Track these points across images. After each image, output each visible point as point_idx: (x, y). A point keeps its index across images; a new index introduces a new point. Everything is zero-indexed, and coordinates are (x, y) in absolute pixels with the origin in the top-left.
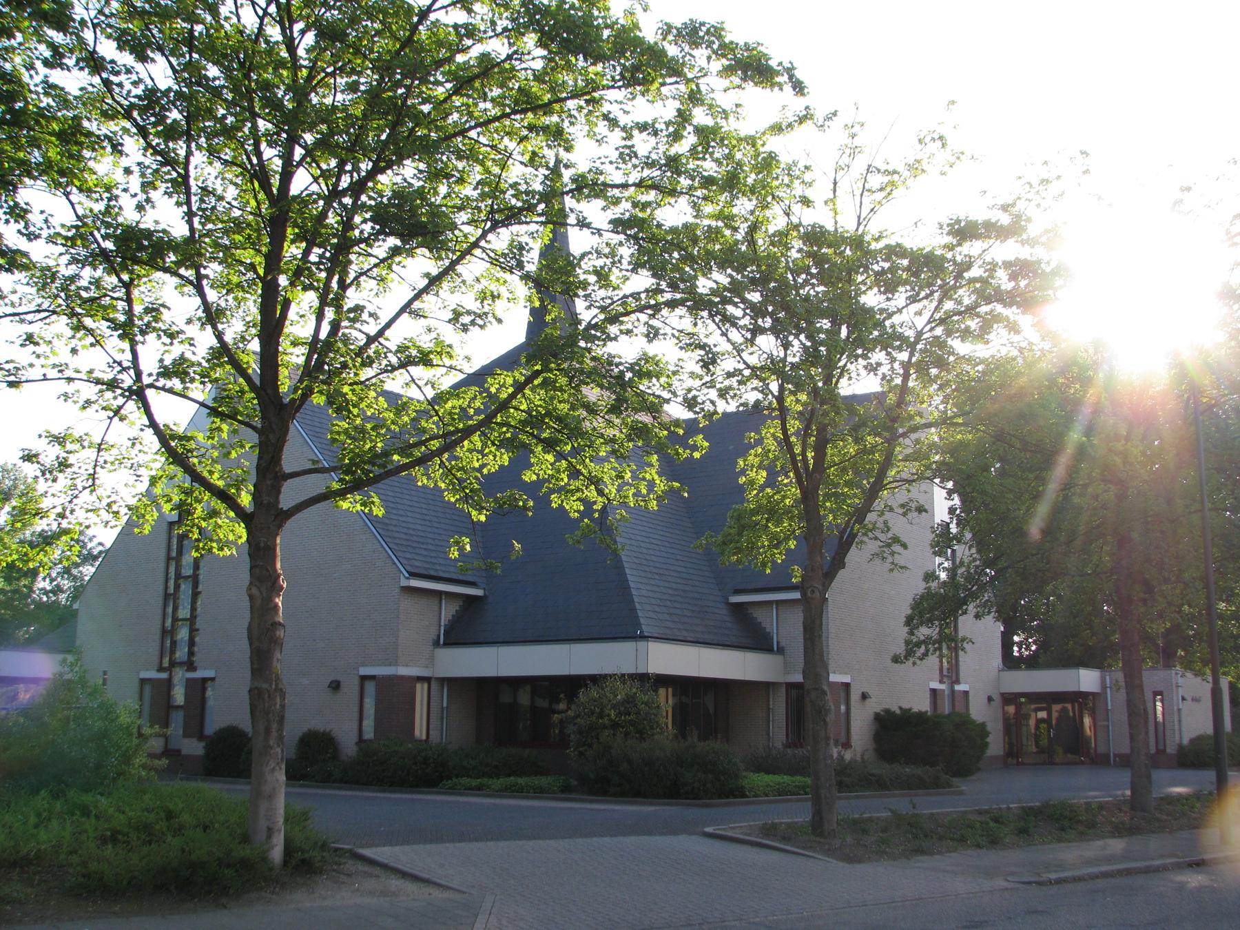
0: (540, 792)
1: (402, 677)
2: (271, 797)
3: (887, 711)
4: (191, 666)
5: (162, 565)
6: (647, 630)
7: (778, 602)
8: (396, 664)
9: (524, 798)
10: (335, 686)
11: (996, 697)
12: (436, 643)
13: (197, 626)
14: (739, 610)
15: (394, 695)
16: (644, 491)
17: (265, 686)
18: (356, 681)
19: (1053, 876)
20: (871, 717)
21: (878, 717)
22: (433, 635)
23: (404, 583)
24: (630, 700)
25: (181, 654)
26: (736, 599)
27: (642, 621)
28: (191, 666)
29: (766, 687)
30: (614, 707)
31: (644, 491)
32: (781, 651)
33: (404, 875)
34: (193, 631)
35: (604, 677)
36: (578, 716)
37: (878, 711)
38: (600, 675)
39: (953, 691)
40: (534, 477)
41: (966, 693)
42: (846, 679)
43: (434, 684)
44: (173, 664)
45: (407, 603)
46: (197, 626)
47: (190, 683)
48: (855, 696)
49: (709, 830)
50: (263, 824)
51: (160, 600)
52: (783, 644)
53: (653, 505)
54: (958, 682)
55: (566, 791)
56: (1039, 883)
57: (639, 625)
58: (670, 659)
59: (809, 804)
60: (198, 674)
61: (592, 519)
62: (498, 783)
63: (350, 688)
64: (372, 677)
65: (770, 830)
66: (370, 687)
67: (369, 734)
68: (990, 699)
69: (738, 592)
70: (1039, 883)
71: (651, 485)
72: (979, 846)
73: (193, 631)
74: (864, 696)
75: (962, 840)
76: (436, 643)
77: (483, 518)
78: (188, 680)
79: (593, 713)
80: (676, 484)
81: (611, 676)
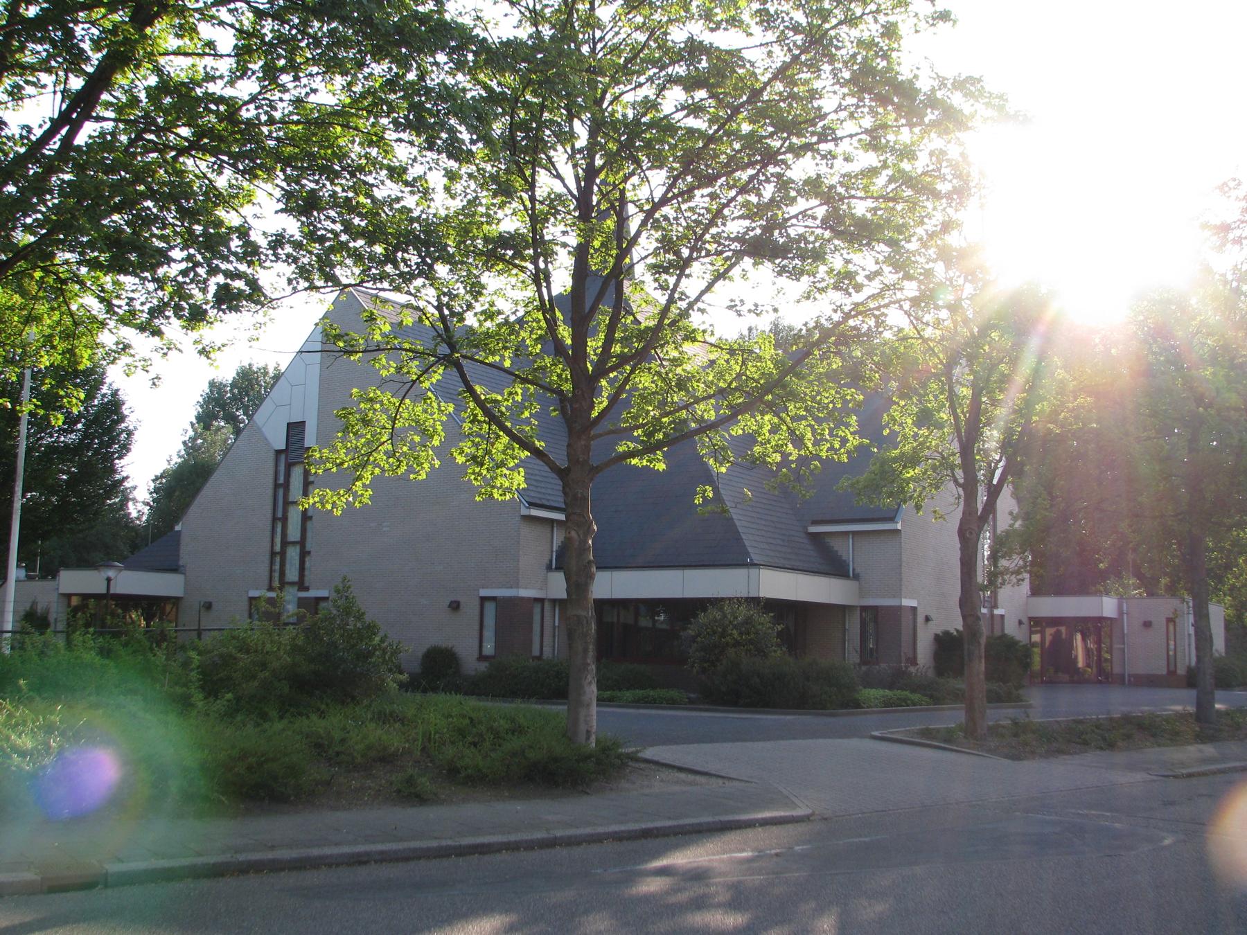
0: (672, 704)
1: (522, 599)
2: (589, 705)
3: (947, 633)
4: (301, 585)
5: (270, 492)
6: (757, 558)
7: (854, 533)
8: (518, 587)
9: (657, 708)
10: (455, 606)
11: (1025, 620)
12: (549, 568)
13: (307, 549)
14: (815, 537)
15: (513, 615)
16: (837, 446)
17: (584, 613)
18: (477, 602)
19: (1184, 771)
20: (931, 637)
21: (937, 638)
22: (546, 561)
23: (524, 512)
24: (748, 621)
25: (292, 574)
26: (813, 529)
27: (750, 550)
28: (301, 585)
29: (843, 609)
30: (735, 627)
31: (837, 446)
32: (856, 577)
33: (680, 769)
34: (304, 554)
35: (722, 599)
36: (699, 635)
37: (939, 632)
38: (716, 599)
39: (992, 615)
40: (740, 432)
41: (1002, 616)
42: (914, 603)
43: (547, 606)
44: (283, 584)
45: (527, 531)
46: (307, 549)
47: (302, 602)
48: (920, 619)
49: (876, 733)
50: (583, 728)
51: (269, 523)
52: (858, 570)
53: (845, 458)
54: (996, 606)
55: (691, 704)
56: (1175, 777)
57: (748, 554)
58: (779, 585)
59: (963, 712)
60: (312, 593)
61: (790, 469)
62: (628, 695)
63: (471, 608)
64: (493, 599)
65: (927, 733)
66: (490, 609)
67: (489, 648)
68: (1020, 623)
69: (815, 523)
70: (1175, 777)
71: (844, 441)
72: (1101, 748)
73: (304, 554)
74: (927, 619)
75: (1086, 743)
76: (549, 568)
77: (723, 470)
78: (300, 599)
79: (715, 633)
80: (866, 441)
81: (730, 599)
